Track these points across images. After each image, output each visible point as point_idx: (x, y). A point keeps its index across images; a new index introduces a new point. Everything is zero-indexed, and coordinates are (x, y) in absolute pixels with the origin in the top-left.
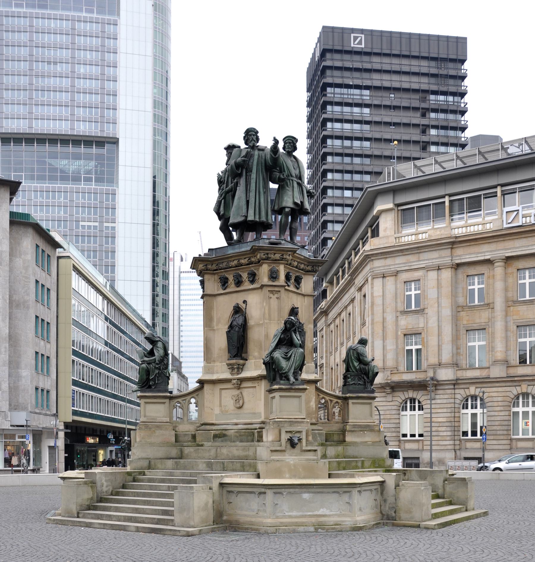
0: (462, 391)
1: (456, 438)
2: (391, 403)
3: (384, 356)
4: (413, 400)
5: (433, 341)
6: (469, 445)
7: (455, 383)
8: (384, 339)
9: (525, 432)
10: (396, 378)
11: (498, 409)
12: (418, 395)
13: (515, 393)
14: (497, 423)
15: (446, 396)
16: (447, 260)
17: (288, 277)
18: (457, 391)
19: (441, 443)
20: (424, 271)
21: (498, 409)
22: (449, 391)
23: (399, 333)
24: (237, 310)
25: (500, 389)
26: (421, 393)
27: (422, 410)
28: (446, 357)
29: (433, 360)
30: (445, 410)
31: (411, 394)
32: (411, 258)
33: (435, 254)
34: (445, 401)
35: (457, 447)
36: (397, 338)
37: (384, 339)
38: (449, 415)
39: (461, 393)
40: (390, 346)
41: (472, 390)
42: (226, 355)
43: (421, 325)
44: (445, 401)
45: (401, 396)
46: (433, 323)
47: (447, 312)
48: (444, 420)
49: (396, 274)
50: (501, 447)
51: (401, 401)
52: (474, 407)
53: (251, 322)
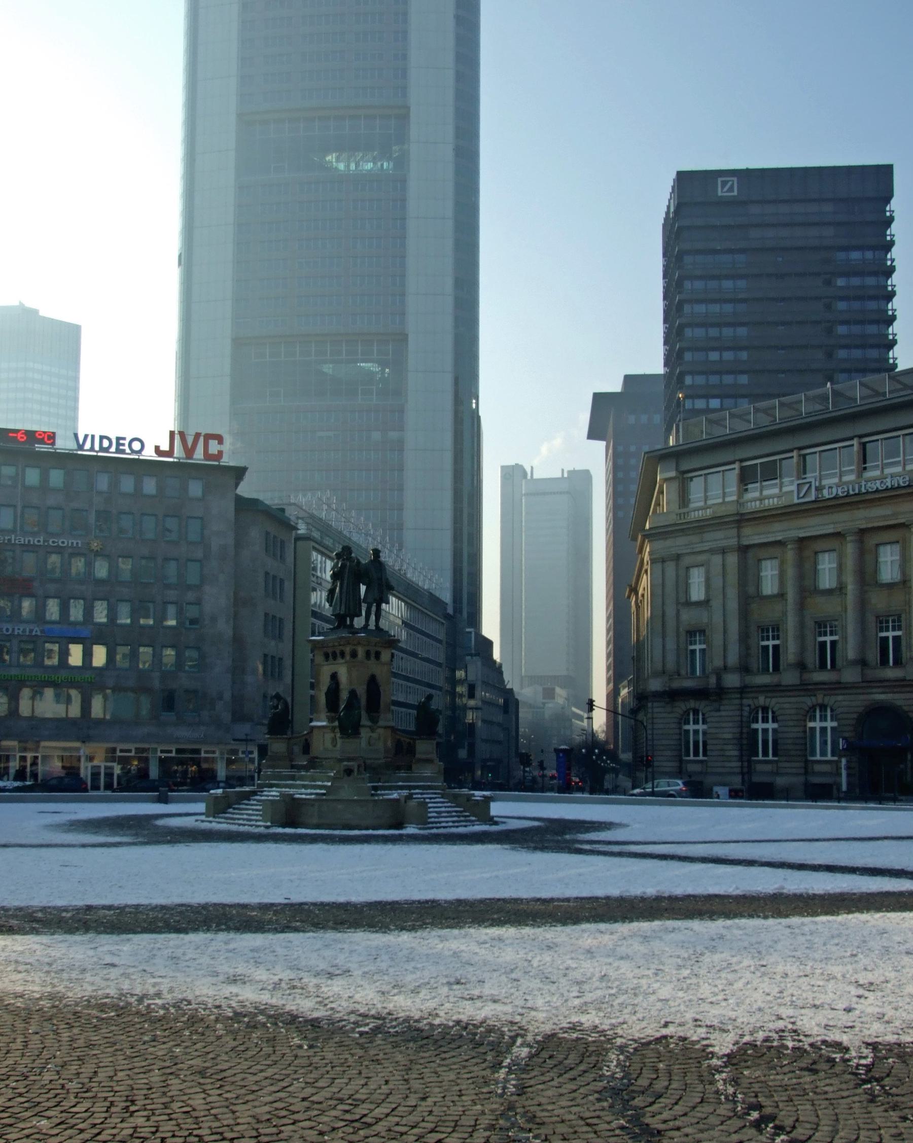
0: (750, 702)
2: (671, 715)
3: (664, 657)
4: (696, 712)
5: (717, 640)
6: (759, 767)
7: (743, 690)
8: (664, 638)
9: (824, 753)
10: (677, 684)
11: (791, 723)
12: (701, 705)
13: (810, 704)
14: (790, 741)
17: (368, 654)
18: (745, 701)
21: (791, 723)
23: (681, 629)
24: (334, 677)
25: (793, 700)
26: (703, 703)
28: (733, 659)
29: (718, 662)
30: (731, 725)
31: (692, 704)
32: (694, 538)
34: (730, 713)
35: (745, 770)
36: (678, 636)
37: (664, 638)
40: (671, 645)
41: (761, 700)
42: (326, 710)
43: (705, 620)
46: (717, 619)
47: (733, 605)
50: (794, 771)
51: (681, 712)
52: (765, 720)
53: (342, 687)
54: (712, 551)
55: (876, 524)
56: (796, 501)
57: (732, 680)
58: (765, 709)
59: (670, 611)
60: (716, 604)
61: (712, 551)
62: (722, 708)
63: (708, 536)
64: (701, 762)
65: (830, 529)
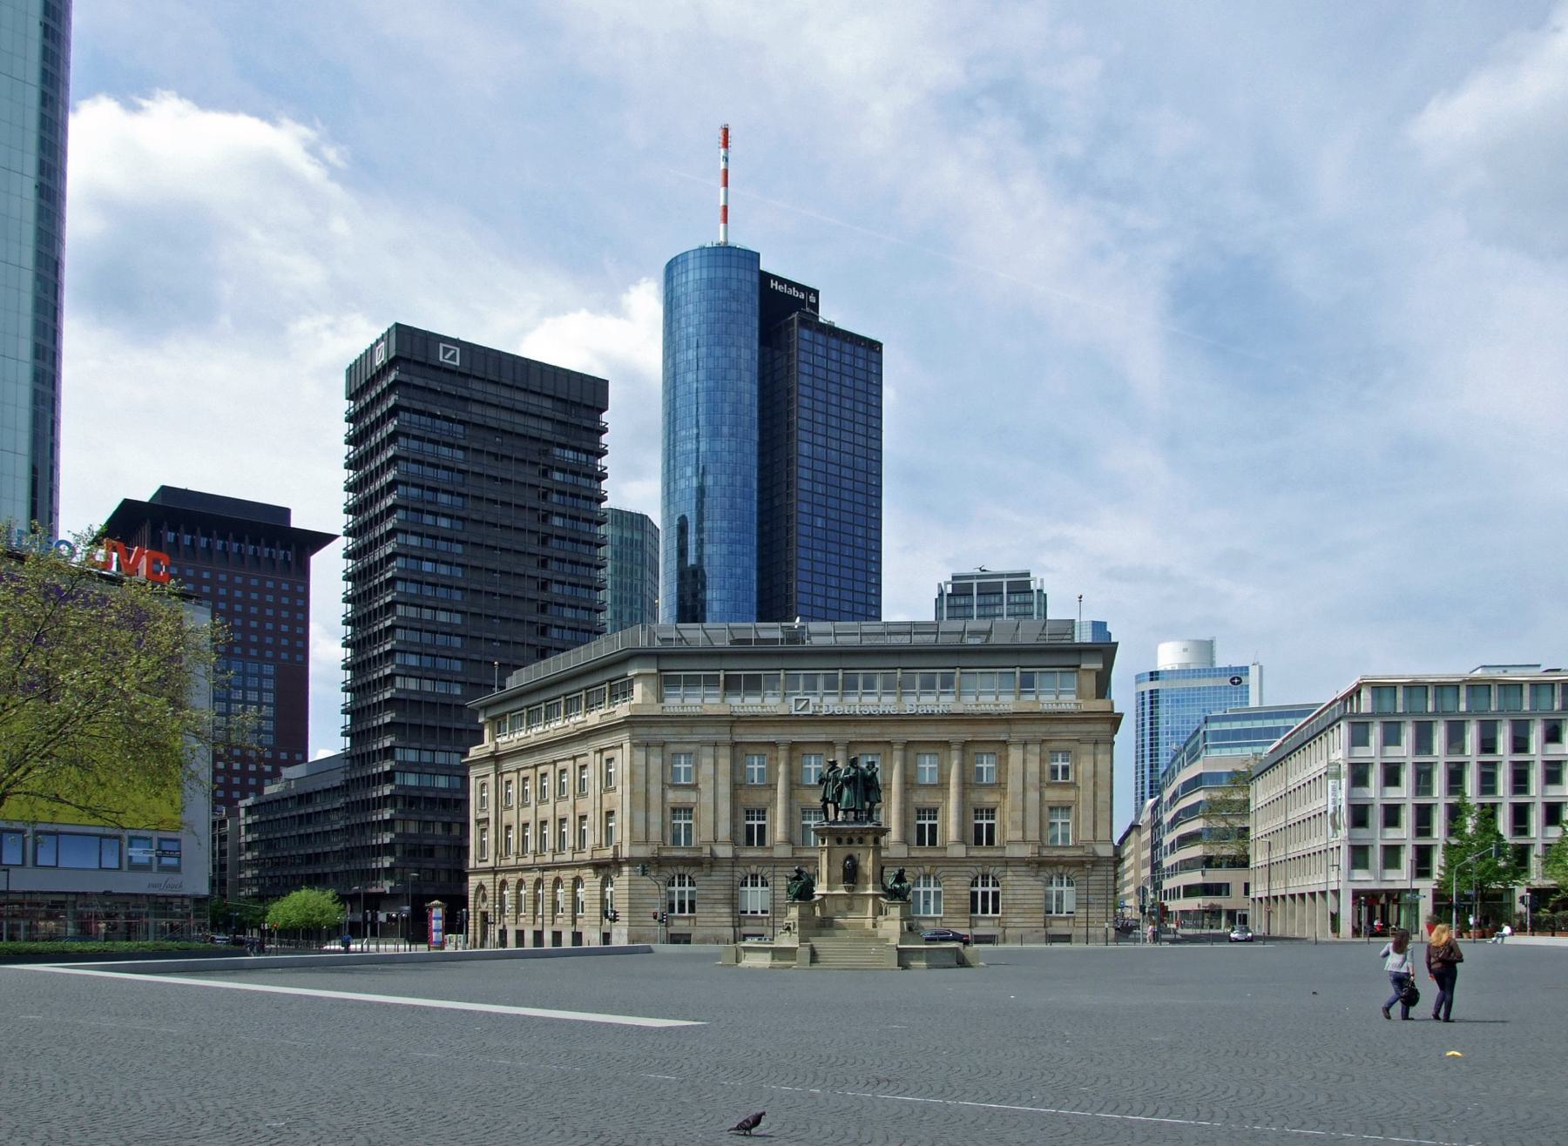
0: (741, 869)
1: (735, 915)
4: (682, 877)
5: (706, 817)
7: (735, 860)
12: (691, 871)
15: (724, 874)
16: (727, 737)
18: (736, 869)
19: (717, 919)
20: (698, 746)
22: (728, 869)
26: (693, 869)
27: (694, 885)
30: (722, 887)
33: (712, 730)
34: (722, 878)
35: (737, 924)
36: (663, 811)
38: (727, 892)
39: (740, 872)
40: (655, 818)
41: (754, 869)
43: (694, 800)
44: (722, 878)
45: (668, 872)
48: (722, 897)
49: (663, 745)
54: (702, 743)
55: (864, 740)
56: (794, 713)
57: (724, 851)
58: (754, 877)
59: (655, 790)
60: (706, 788)
61: (702, 743)
62: (713, 873)
63: (700, 730)
64: (689, 918)
65: (822, 738)
